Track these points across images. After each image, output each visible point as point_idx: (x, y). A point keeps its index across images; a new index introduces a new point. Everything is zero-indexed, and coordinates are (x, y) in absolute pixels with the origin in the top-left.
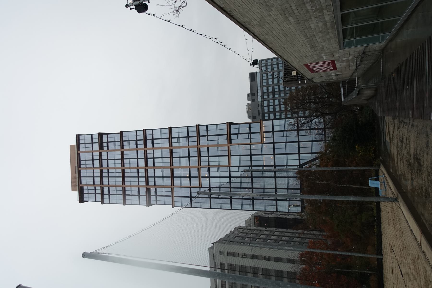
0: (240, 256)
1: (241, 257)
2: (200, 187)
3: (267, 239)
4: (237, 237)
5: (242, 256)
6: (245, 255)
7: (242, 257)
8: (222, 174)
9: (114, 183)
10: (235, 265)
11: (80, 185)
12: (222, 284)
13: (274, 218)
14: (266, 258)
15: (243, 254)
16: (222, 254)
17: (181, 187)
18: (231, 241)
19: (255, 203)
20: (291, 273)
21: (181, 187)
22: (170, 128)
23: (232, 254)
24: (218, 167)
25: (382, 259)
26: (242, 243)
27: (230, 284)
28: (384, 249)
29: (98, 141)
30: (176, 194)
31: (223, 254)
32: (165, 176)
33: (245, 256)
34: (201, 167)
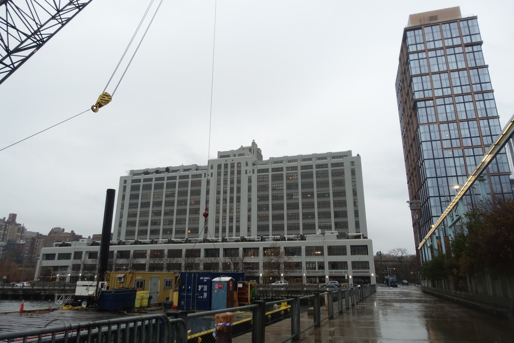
0: (353, 180)
1: (352, 181)
2: (443, 149)
7: (352, 182)
8: (458, 169)
9: (431, 63)
11: (423, 27)
12: (324, 165)
14: (356, 203)
15: (355, 183)
16: (352, 164)
17: (440, 131)
19: (436, 198)
20: (347, 224)
21: (440, 131)
22: (497, 117)
24: (465, 165)
27: (325, 172)
29: (473, 42)
30: (431, 126)
32: (448, 114)
33: (353, 184)
34: (462, 149)
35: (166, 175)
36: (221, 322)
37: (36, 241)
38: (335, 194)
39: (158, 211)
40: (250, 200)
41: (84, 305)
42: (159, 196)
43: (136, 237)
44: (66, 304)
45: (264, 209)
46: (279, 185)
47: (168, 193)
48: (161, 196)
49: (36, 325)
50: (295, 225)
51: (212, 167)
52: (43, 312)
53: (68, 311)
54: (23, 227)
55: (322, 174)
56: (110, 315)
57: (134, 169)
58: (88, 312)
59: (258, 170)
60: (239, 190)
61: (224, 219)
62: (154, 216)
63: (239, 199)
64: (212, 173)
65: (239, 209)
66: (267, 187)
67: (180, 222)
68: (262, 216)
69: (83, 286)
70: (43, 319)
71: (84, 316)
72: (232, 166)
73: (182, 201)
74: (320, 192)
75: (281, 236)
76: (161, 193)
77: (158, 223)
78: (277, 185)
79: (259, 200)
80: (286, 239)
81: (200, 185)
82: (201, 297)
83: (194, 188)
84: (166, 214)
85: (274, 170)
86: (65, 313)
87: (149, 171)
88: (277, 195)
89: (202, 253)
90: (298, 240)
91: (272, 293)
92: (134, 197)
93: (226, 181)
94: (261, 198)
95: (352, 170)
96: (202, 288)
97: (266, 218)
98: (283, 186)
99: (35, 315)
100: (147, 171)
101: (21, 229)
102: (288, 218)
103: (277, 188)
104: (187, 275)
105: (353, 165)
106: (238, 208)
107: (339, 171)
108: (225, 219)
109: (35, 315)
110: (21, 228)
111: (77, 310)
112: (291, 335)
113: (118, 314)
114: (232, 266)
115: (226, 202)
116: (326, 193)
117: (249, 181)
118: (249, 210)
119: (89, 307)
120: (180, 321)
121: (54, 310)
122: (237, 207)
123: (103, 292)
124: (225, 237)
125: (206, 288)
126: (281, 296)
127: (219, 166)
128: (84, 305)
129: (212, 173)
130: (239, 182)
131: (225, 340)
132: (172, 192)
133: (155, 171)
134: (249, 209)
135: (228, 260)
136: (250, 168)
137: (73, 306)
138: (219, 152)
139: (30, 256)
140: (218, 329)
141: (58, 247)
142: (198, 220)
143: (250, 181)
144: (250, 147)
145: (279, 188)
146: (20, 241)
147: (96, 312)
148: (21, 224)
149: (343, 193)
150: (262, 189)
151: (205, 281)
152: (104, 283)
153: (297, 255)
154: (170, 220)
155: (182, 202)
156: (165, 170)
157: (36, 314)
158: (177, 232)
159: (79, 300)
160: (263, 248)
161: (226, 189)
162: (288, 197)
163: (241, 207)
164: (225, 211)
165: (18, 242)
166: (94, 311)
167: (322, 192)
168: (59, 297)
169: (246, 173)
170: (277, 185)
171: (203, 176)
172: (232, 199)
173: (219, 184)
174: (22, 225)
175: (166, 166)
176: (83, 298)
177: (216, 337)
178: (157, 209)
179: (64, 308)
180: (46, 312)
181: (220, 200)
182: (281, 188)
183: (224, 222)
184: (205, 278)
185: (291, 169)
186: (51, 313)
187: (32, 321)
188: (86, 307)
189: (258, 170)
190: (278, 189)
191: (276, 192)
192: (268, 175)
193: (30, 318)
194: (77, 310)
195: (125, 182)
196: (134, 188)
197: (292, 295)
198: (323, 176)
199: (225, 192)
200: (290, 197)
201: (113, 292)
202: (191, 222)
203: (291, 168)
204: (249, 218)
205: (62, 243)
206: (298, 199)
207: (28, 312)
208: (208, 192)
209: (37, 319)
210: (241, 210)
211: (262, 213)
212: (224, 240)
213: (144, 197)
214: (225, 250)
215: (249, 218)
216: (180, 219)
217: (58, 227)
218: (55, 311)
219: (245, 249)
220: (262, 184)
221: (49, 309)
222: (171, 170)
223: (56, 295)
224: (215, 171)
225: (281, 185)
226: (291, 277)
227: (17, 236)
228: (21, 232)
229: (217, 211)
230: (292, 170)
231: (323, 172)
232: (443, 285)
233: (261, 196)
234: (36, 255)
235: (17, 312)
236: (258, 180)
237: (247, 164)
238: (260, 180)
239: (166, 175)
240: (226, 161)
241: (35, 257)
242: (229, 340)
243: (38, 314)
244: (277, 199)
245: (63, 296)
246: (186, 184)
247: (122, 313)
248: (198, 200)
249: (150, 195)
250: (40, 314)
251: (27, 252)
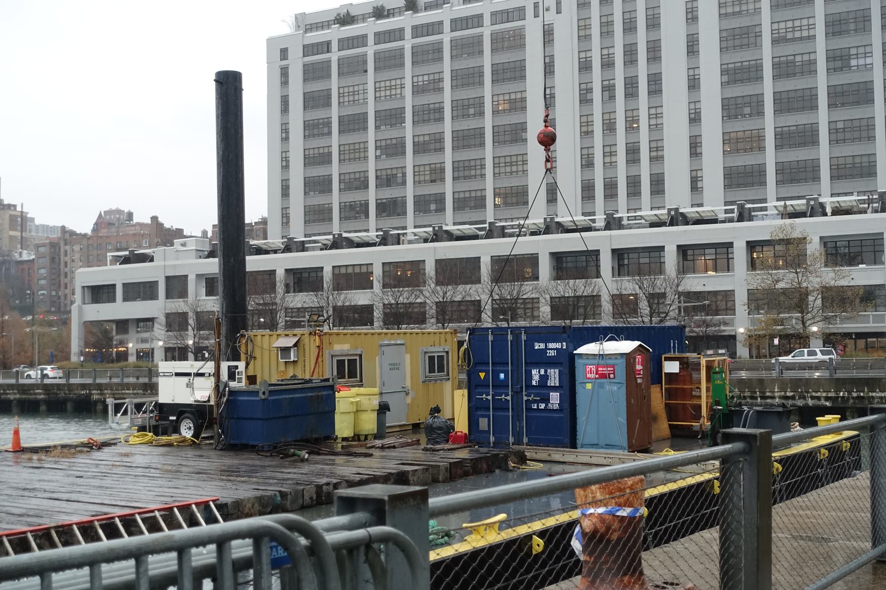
36: (596, 503)
37: (62, 250)
39: (394, 141)
40: (694, 84)
41: (187, 431)
42: (393, 92)
43: (336, 227)
44: (142, 429)
45: (747, 110)
46: (797, 23)
47: (420, 78)
48: (399, 91)
49: (45, 491)
50: (858, 160)
52: (73, 451)
53: (146, 449)
54: (22, 212)
56: (258, 463)
58: (198, 453)
60: (654, 52)
61: (609, 152)
62: (384, 157)
63: (655, 84)
65: (657, 116)
66: (754, 35)
67: (467, 173)
68: (740, 135)
69: (177, 374)
70: (70, 472)
71: (184, 463)
73: (466, 103)
75: (809, 200)
76: (398, 82)
77: (400, 180)
78: (790, 24)
79: (728, 83)
80: (829, 210)
81: (523, 46)
82: (542, 406)
83: (505, 57)
84: (420, 148)
86: (133, 454)
87: (353, 13)
88: (792, 57)
89: (545, 268)
90: (870, 210)
91: (783, 389)
93: (610, 24)
96: (544, 378)
97: (755, 142)
99: (50, 459)
101: (19, 219)
102: (834, 137)
103: (790, 36)
104: (490, 338)
106: (655, 115)
108: (612, 154)
109: (48, 461)
110: (16, 216)
111: (169, 445)
112: (869, 545)
113: (282, 458)
114: (644, 306)
115: (612, 97)
117: (690, 16)
118: (695, 118)
119: (203, 435)
120: (385, 539)
121: (104, 446)
122: (653, 111)
123: (232, 393)
124: (617, 211)
125: (554, 376)
126: (812, 398)
128: (187, 431)
131: (615, 562)
132: (432, 77)
134: (692, 116)
135: (629, 286)
137: (156, 434)
139: (54, 293)
140: (587, 530)
141: (118, 266)
142: (525, 162)
145: (797, 34)
146: (21, 254)
147: (220, 453)
148: (15, 206)
150: (737, 42)
151: (552, 353)
152: (237, 367)
153: (867, 264)
154: (433, 166)
155: (469, 106)
157: (54, 457)
158: (460, 204)
159: (171, 418)
160: (748, 243)
161: (611, 51)
162: (832, 65)
163: (665, 110)
164: (609, 127)
165: (17, 256)
166: (215, 449)
168: (117, 408)
170: (790, 24)
171: (530, 12)
172: (632, 84)
173: (584, 38)
174: (19, 209)
176: (181, 410)
177: (584, 551)
178: (390, 133)
179: (132, 440)
180: (81, 452)
181: (590, 90)
182: (805, 34)
183: (609, 165)
184: (551, 345)
186: (97, 455)
187: (38, 478)
188: (192, 437)
190: (794, 40)
193: (36, 471)
194: (169, 445)
195: (284, 53)
197: (850, 393)
199: (608, 64)
201: (264, 393)
202: (502, 170)
204: (695, 148)
205: (127, 253)
206: (869, 68)
207: (31, 452)
208: (549, 69)
209: (52, 472)
210: (665, 120)
211: (740, 126)
212: (612, 223)
213: (346, 99)
214: (619, 254)
215: (695, 148)
216: (467, 164)
217: (114, 208)
218: (106, 450)
219: (683, 250)
220: (735, 23)
221: (89, 443)
223: (110, 401)
225: (805, 22)
226: (848, 335)
227: (11, 237)
228: (19, 228)
229: (584, 129)
233: (735, 69)
234: (67, 291)
235: (6, 451)
236: (723, 11)
238: (730, 10)
241: (66, 295)
242: (633, 560)
243: (58, 457)
245: (127, 406)
246: (472, 47)
247: (294, 455)
248: (519, 96)
249: (365, 92)
250: (63, 457)
251: (43, 282)
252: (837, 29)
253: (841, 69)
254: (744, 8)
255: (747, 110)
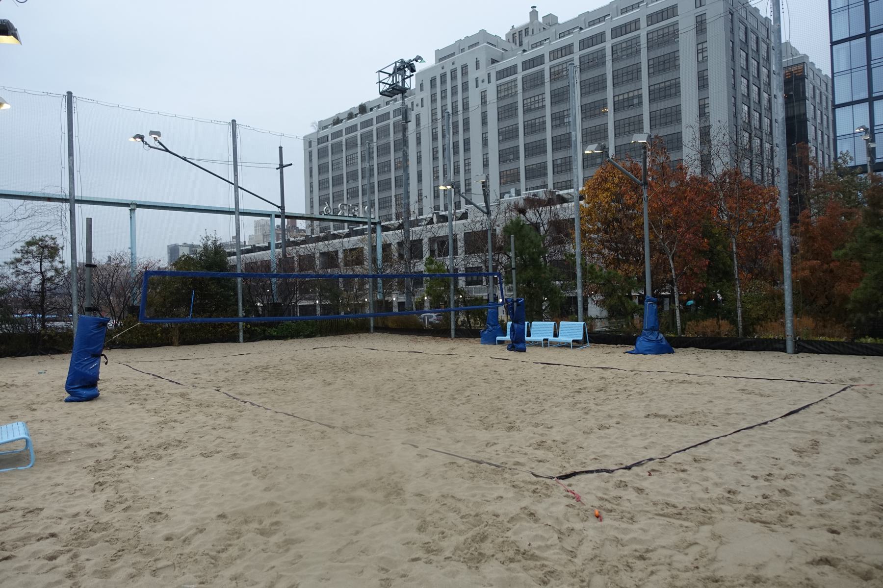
0: (700, 47)
3: (750, 103)
4: (746, 28)
5: (701, 51)
6: (703, 58)
7: (698, 53)
10: (678, 41)
12: (630, 23)
13: (805, 114)
14: (705, 107)
18: (732, 15)
23: (701, 26)
25: (784, 350)
26: (733, 43)
28: (816, 358)
31: (698, 5)
33: (700, 59)
35: (357, 120)
38: (655, 96)
40: (485, 143)
46: (537, 98)
51: (422, 85)
55: (627, 48)
57: (323, 119)
59: (497, 73)
63: (467, 142)
64: (422, 99)
65: (469, 164)
72: (454, 77)
74: (621, 97)
78: (533, 99)
85: (527, 65)
87: (341, 119)
92: (322, 169)
94: (508, 134)
95: (699, 19)
98: (543, 100)
100: (338, 119)
103: (533, 107)
105: (703, 4)
106: (467, 164)
107: (666, 31)
116: (633, 98)
127: (433, 81)
129: (422, 99)
130: (466, 108)
133: (346, 116)
136: (482, 74)
138: (437, 51)
143: (484, 102)
144: (528, 25)
145: (537, 106)
149: (672, 90)
156: (358, 111)
167: (626, 96)
169: (477, 86)
170: (533, 99)
175: (357, 105)
178: (353, 185)
181: (437, 152)
182: (541, 105)
185: (560, 55)
189: (497, 73)
190: (535, 109)
191: (531, 116)
192: (516, 80)
195: (310, 143)
196: (322, 153)
198: (627, 55)
200: (558, 122)
203: (560, 53)
222: (368, 108)
224: (426, 94)
225: (540, 97)
230: (562, 57)
231: (629, 43)
232: (678, 321)
237: (477, 67)
238: (503, 95)
239: (357, 120)
240: (443, 68)
244: (534, 132)
252: (557, 99)
253: (560, 125)
254: (510, 92)
255: (512, 157)
